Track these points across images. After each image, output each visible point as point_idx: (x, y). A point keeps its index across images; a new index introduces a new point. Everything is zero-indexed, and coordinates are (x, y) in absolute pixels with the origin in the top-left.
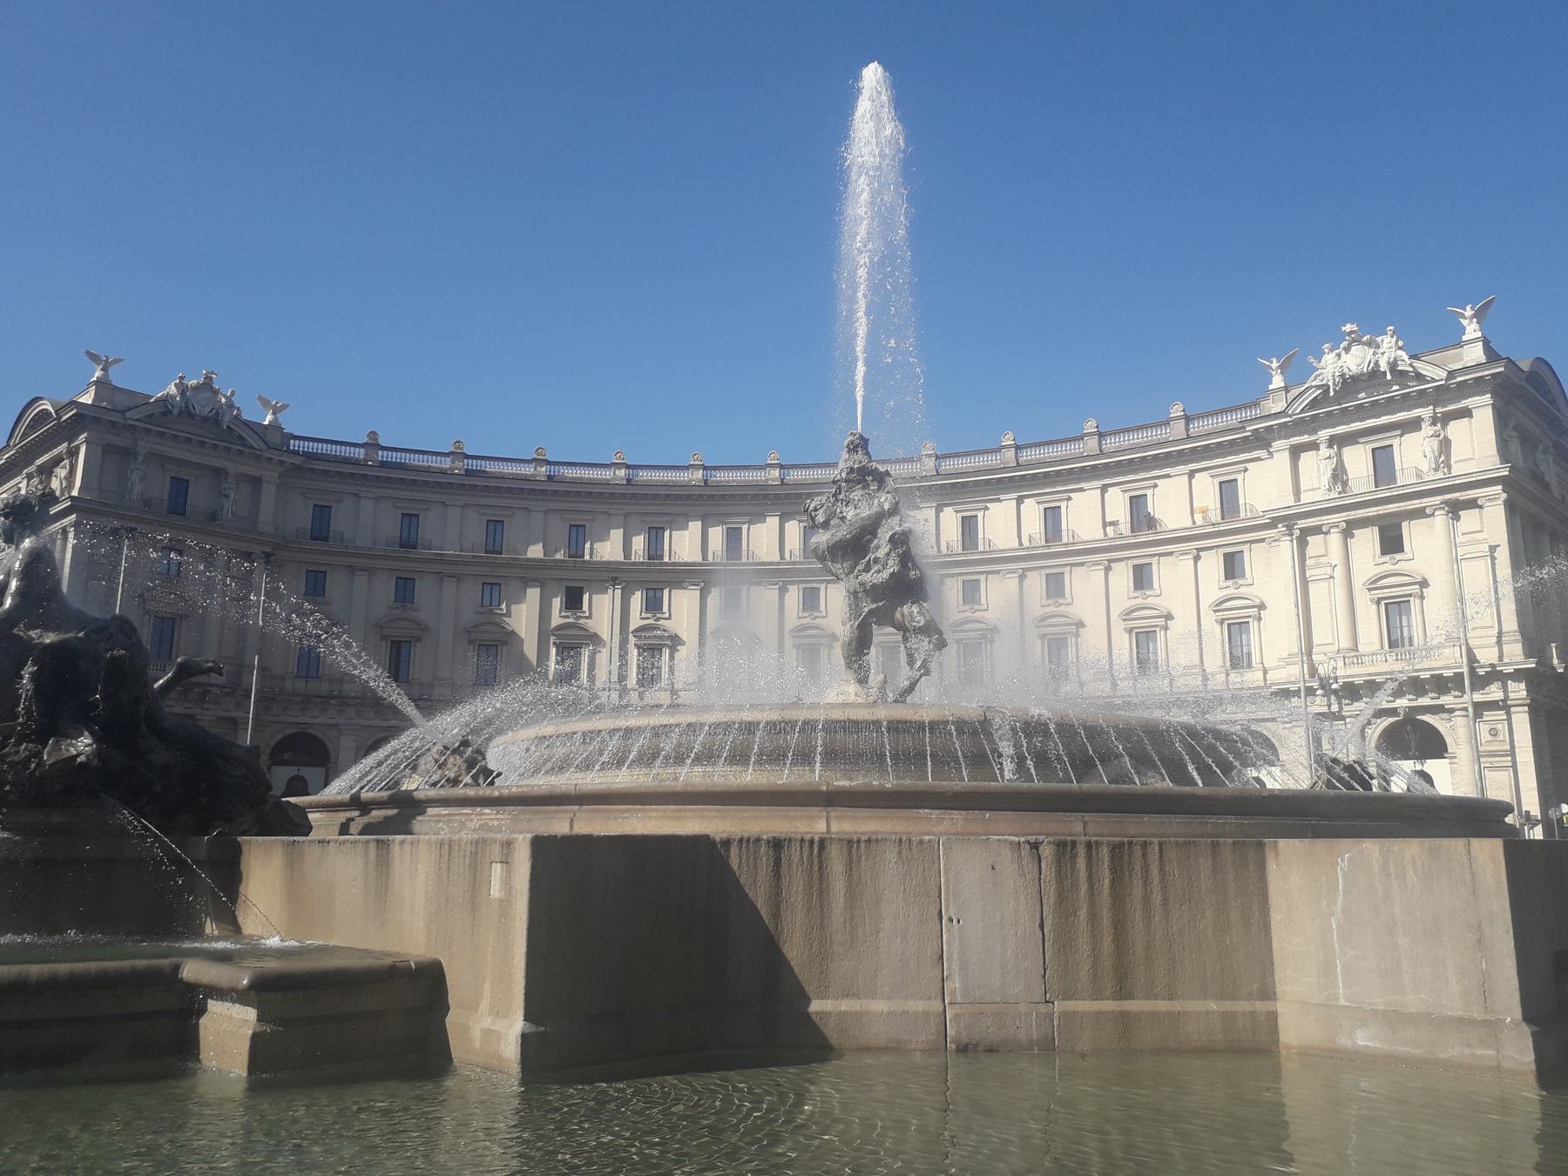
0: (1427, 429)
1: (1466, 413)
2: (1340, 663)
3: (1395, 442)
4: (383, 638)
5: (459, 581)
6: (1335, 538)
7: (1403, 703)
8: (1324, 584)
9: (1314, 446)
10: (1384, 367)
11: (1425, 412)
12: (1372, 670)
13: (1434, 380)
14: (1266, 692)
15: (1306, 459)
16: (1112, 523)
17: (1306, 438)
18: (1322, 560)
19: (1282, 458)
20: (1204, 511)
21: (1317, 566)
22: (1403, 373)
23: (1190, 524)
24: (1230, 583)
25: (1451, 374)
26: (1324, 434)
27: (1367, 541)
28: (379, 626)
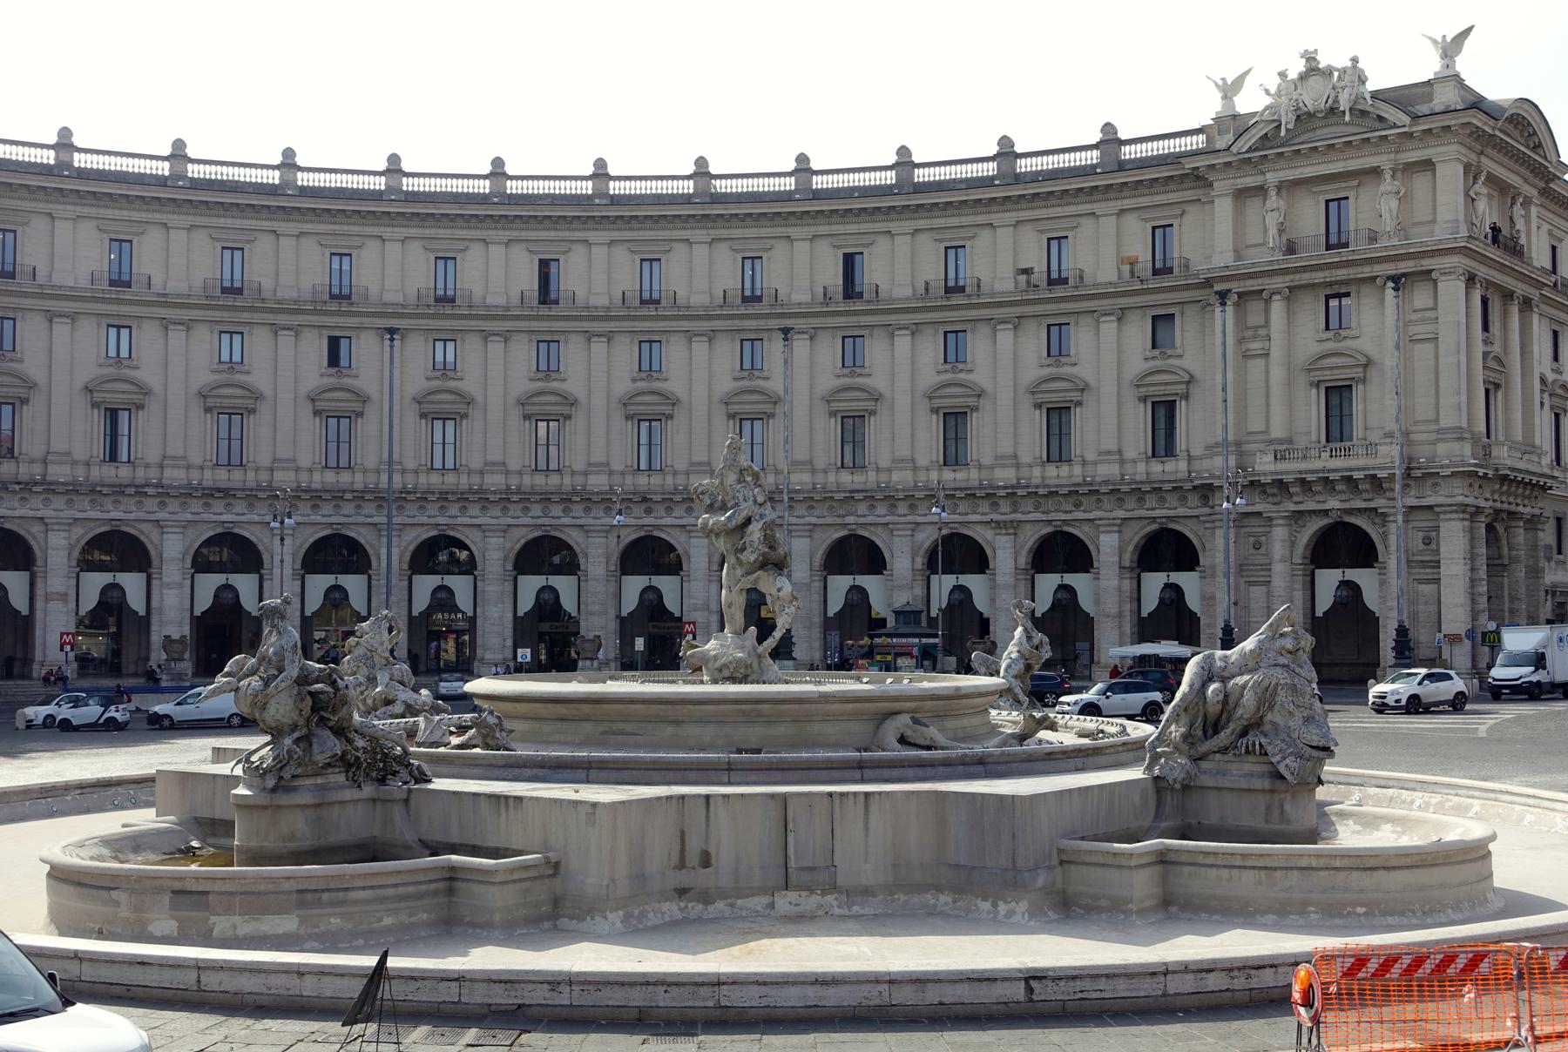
0: (1388, 184)
2: (1271, 458)
4: (95, 405)
5: (188, 329)
6: (1277, 307)
7: (1333, 503)
8: (1261, 362)
9: (1261, 191)
10: (1344, 105)
11: (1383, 160)
12: (1303, 466)
13: (1395, 126)
14: (1188, 486)
15: (1253, 206)
16: (1027, 271)
17: (1251, 181)
18: (1262, 332)
19: (1224, 207)
20: (1133, 263)
21: (1255, 337)
22: (1364, 113)
23: (1114, 278)
24: (1156, 352)
25: (1416, 118)
26: (1272, 178)
27: (1310, 315)
28: (88, 389)
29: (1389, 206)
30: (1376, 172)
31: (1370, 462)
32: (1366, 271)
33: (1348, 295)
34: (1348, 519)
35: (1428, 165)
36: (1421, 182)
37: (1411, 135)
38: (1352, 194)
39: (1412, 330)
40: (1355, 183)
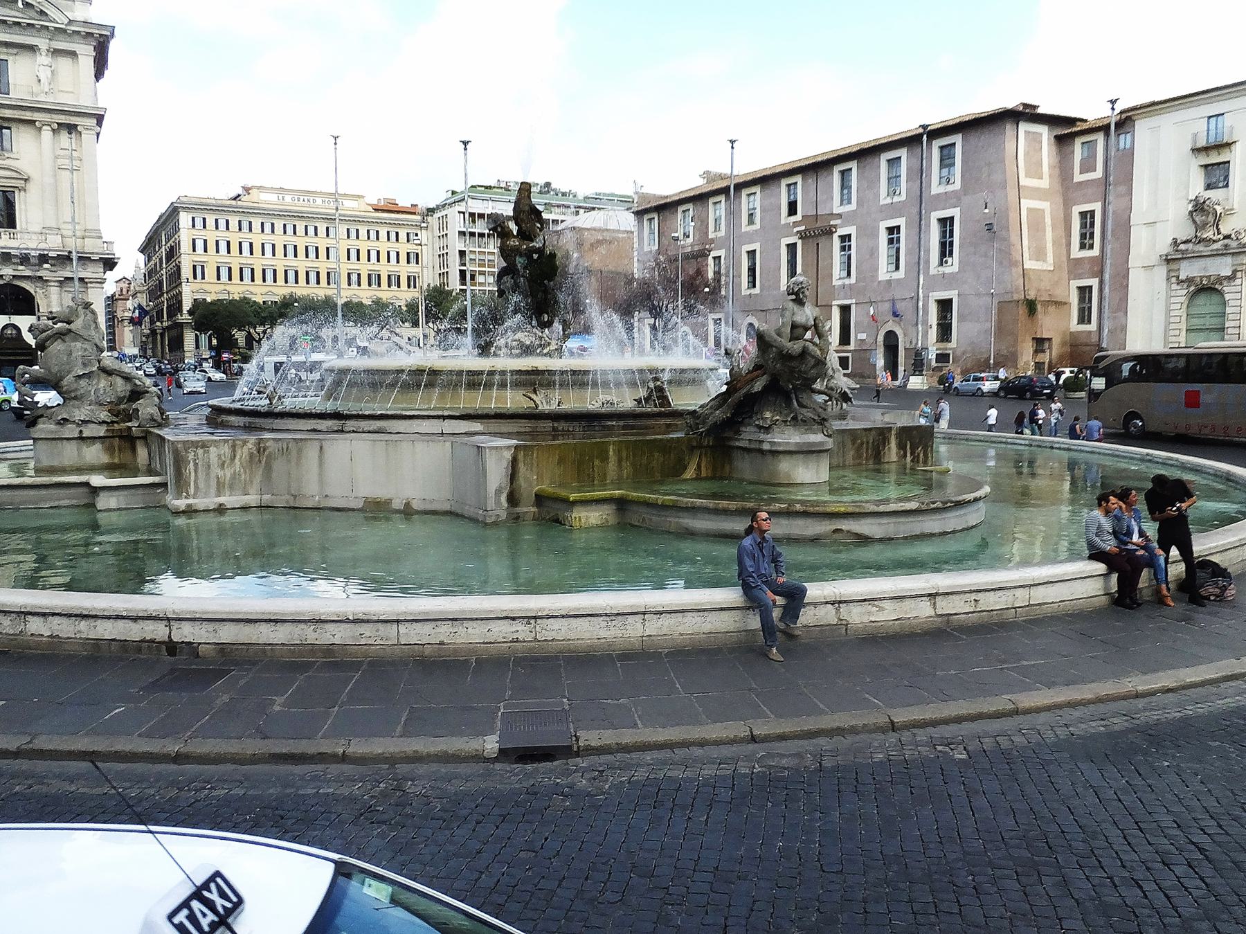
0: (43, 59)
1: (73, 54)
3: (10, 59)
11: (42, 43)
13: (54, 21)
25: (71, 22)
29: (45, 74)
30: (32, 49)
31: (42, 246)
32: (28, 115)
33: (9, 128)
34: (19, 283)
35: (73, 54)
36: (64, 63)
37: (65, 31)
38: (10, 59)
39: (60, 161)
40: (15, 51)
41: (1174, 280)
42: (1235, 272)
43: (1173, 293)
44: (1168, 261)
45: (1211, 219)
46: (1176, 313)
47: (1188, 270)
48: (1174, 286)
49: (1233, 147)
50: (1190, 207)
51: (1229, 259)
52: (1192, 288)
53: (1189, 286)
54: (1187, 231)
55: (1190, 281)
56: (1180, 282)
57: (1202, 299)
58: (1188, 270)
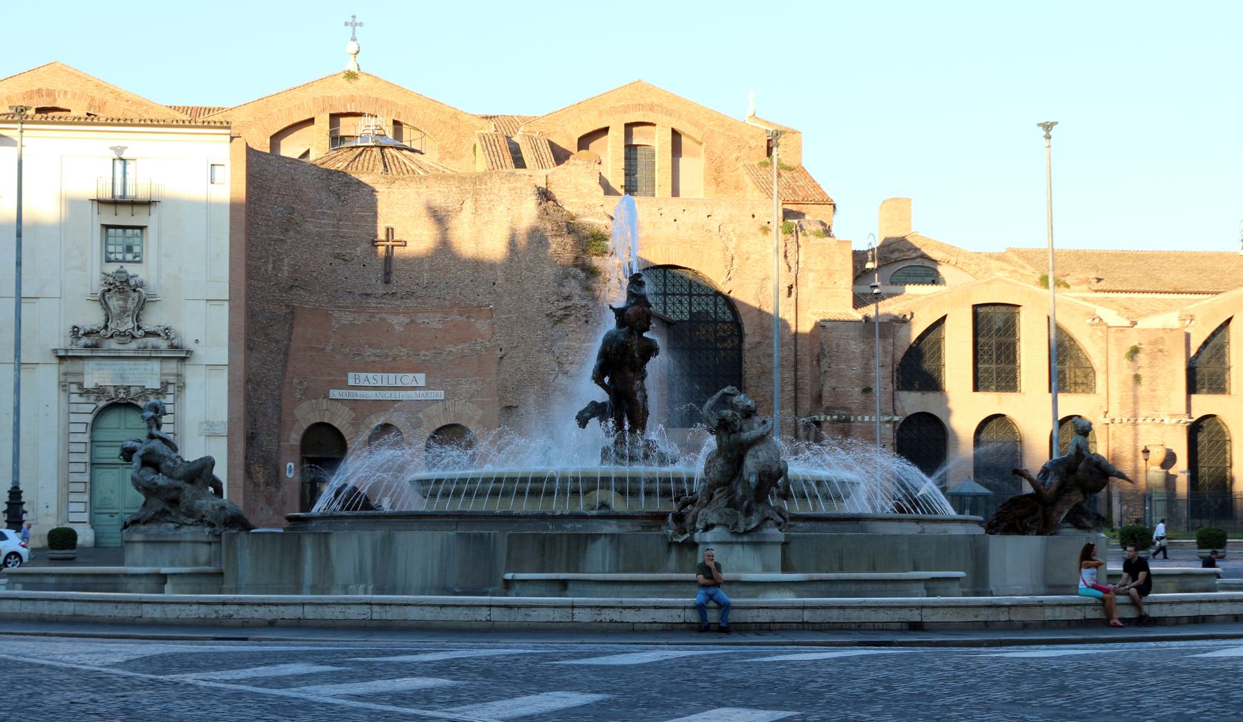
41: (74, 388)
42: (165, 385)
43: (73, 408)
44: (61, 358)
45: (131, 305)
46: (80, 438)
47: (98, 375)
48: (75, 398)
49: (153, 208)
50: (98, 288)
51: (156, 366)
52: (102, 404)
53: (98, 399)
54: (92, 318)
55: (100, 391)
56: (84, 392)
57: (112, 419)
58: (98, 375)
